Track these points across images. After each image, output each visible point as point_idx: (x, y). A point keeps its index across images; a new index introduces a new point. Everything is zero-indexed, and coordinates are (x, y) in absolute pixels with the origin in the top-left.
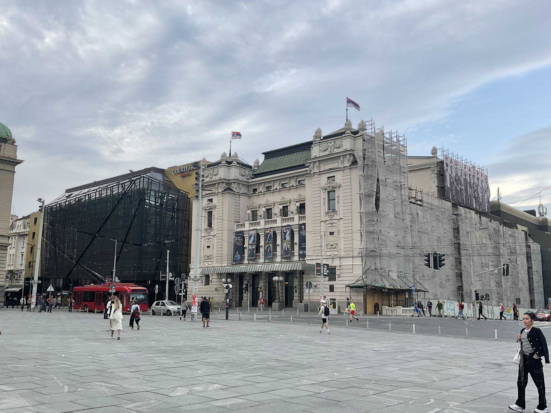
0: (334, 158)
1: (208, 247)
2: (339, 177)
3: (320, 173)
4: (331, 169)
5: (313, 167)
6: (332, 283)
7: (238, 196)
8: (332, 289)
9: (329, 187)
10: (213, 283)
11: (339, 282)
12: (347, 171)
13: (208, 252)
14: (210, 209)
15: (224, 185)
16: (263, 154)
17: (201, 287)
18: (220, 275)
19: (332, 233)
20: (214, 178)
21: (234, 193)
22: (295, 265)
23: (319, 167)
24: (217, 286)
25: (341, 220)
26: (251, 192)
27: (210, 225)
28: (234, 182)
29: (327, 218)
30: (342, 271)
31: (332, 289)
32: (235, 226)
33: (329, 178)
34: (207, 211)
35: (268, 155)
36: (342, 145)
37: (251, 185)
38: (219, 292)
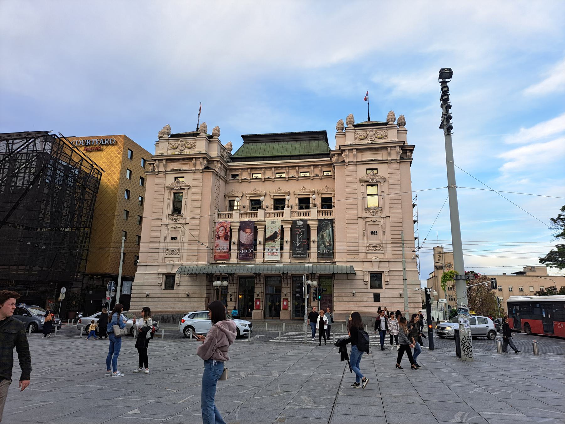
0: (371, 148)
1: (173, 238)
2: (383, 171)
3: (358, 163)
4: (372, 160)
5: (347, 156)
6: (377, 291)
7: (218, 178)
8: (377, 298)
9: (373, 179)
10: (180, 287)
11: (387, 291)
12: (394, 164)
13: (174, 245)
14: (181, 189)
15: (205, 162)
16: (243, 137)
17: (158, 291)
18: (194, 276)
19: (373, 233)
20: (187, 151)
21: (216, 174)
22: (325, 268)
23: (355, 156)
24: (190, 291)
25: (388, 219)
26: (230, 177)
27: (177, 209)
28: (218, 161)
29: (368, 215)
30: (392, 278)
31: (377, 298)
32: (216, 216)
33: (367, 169)
34: (173, 192)
35: (247, 138)
36: (386, 136)
37: (230, 169)
38: (192, 300)
